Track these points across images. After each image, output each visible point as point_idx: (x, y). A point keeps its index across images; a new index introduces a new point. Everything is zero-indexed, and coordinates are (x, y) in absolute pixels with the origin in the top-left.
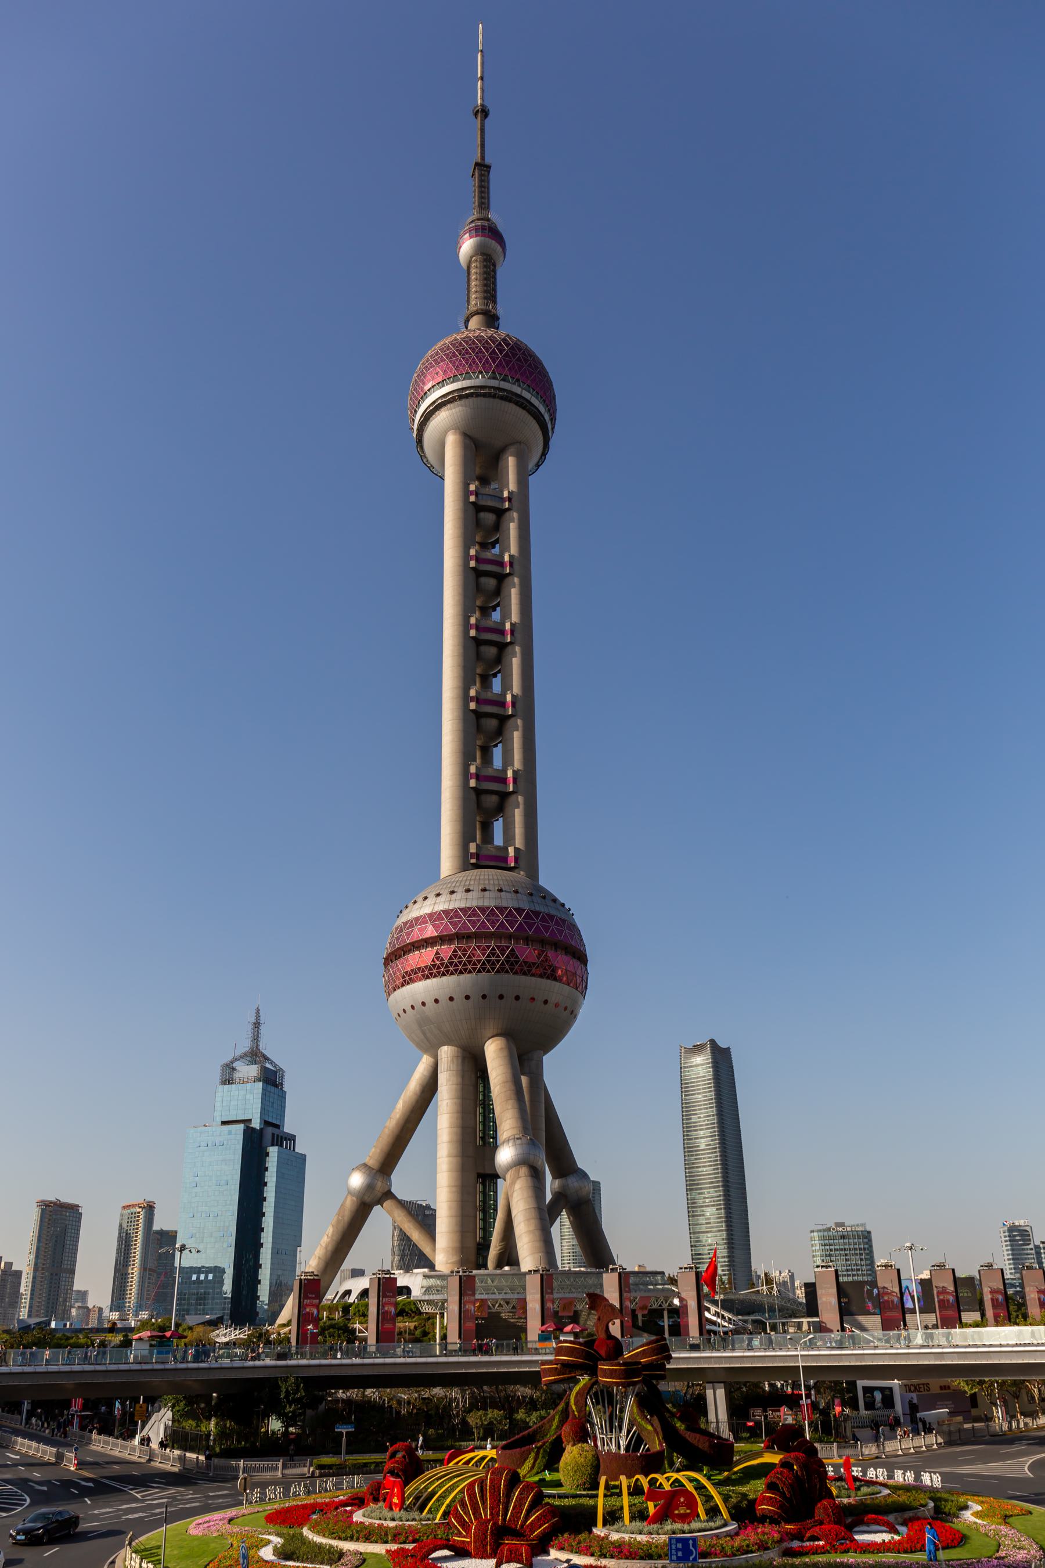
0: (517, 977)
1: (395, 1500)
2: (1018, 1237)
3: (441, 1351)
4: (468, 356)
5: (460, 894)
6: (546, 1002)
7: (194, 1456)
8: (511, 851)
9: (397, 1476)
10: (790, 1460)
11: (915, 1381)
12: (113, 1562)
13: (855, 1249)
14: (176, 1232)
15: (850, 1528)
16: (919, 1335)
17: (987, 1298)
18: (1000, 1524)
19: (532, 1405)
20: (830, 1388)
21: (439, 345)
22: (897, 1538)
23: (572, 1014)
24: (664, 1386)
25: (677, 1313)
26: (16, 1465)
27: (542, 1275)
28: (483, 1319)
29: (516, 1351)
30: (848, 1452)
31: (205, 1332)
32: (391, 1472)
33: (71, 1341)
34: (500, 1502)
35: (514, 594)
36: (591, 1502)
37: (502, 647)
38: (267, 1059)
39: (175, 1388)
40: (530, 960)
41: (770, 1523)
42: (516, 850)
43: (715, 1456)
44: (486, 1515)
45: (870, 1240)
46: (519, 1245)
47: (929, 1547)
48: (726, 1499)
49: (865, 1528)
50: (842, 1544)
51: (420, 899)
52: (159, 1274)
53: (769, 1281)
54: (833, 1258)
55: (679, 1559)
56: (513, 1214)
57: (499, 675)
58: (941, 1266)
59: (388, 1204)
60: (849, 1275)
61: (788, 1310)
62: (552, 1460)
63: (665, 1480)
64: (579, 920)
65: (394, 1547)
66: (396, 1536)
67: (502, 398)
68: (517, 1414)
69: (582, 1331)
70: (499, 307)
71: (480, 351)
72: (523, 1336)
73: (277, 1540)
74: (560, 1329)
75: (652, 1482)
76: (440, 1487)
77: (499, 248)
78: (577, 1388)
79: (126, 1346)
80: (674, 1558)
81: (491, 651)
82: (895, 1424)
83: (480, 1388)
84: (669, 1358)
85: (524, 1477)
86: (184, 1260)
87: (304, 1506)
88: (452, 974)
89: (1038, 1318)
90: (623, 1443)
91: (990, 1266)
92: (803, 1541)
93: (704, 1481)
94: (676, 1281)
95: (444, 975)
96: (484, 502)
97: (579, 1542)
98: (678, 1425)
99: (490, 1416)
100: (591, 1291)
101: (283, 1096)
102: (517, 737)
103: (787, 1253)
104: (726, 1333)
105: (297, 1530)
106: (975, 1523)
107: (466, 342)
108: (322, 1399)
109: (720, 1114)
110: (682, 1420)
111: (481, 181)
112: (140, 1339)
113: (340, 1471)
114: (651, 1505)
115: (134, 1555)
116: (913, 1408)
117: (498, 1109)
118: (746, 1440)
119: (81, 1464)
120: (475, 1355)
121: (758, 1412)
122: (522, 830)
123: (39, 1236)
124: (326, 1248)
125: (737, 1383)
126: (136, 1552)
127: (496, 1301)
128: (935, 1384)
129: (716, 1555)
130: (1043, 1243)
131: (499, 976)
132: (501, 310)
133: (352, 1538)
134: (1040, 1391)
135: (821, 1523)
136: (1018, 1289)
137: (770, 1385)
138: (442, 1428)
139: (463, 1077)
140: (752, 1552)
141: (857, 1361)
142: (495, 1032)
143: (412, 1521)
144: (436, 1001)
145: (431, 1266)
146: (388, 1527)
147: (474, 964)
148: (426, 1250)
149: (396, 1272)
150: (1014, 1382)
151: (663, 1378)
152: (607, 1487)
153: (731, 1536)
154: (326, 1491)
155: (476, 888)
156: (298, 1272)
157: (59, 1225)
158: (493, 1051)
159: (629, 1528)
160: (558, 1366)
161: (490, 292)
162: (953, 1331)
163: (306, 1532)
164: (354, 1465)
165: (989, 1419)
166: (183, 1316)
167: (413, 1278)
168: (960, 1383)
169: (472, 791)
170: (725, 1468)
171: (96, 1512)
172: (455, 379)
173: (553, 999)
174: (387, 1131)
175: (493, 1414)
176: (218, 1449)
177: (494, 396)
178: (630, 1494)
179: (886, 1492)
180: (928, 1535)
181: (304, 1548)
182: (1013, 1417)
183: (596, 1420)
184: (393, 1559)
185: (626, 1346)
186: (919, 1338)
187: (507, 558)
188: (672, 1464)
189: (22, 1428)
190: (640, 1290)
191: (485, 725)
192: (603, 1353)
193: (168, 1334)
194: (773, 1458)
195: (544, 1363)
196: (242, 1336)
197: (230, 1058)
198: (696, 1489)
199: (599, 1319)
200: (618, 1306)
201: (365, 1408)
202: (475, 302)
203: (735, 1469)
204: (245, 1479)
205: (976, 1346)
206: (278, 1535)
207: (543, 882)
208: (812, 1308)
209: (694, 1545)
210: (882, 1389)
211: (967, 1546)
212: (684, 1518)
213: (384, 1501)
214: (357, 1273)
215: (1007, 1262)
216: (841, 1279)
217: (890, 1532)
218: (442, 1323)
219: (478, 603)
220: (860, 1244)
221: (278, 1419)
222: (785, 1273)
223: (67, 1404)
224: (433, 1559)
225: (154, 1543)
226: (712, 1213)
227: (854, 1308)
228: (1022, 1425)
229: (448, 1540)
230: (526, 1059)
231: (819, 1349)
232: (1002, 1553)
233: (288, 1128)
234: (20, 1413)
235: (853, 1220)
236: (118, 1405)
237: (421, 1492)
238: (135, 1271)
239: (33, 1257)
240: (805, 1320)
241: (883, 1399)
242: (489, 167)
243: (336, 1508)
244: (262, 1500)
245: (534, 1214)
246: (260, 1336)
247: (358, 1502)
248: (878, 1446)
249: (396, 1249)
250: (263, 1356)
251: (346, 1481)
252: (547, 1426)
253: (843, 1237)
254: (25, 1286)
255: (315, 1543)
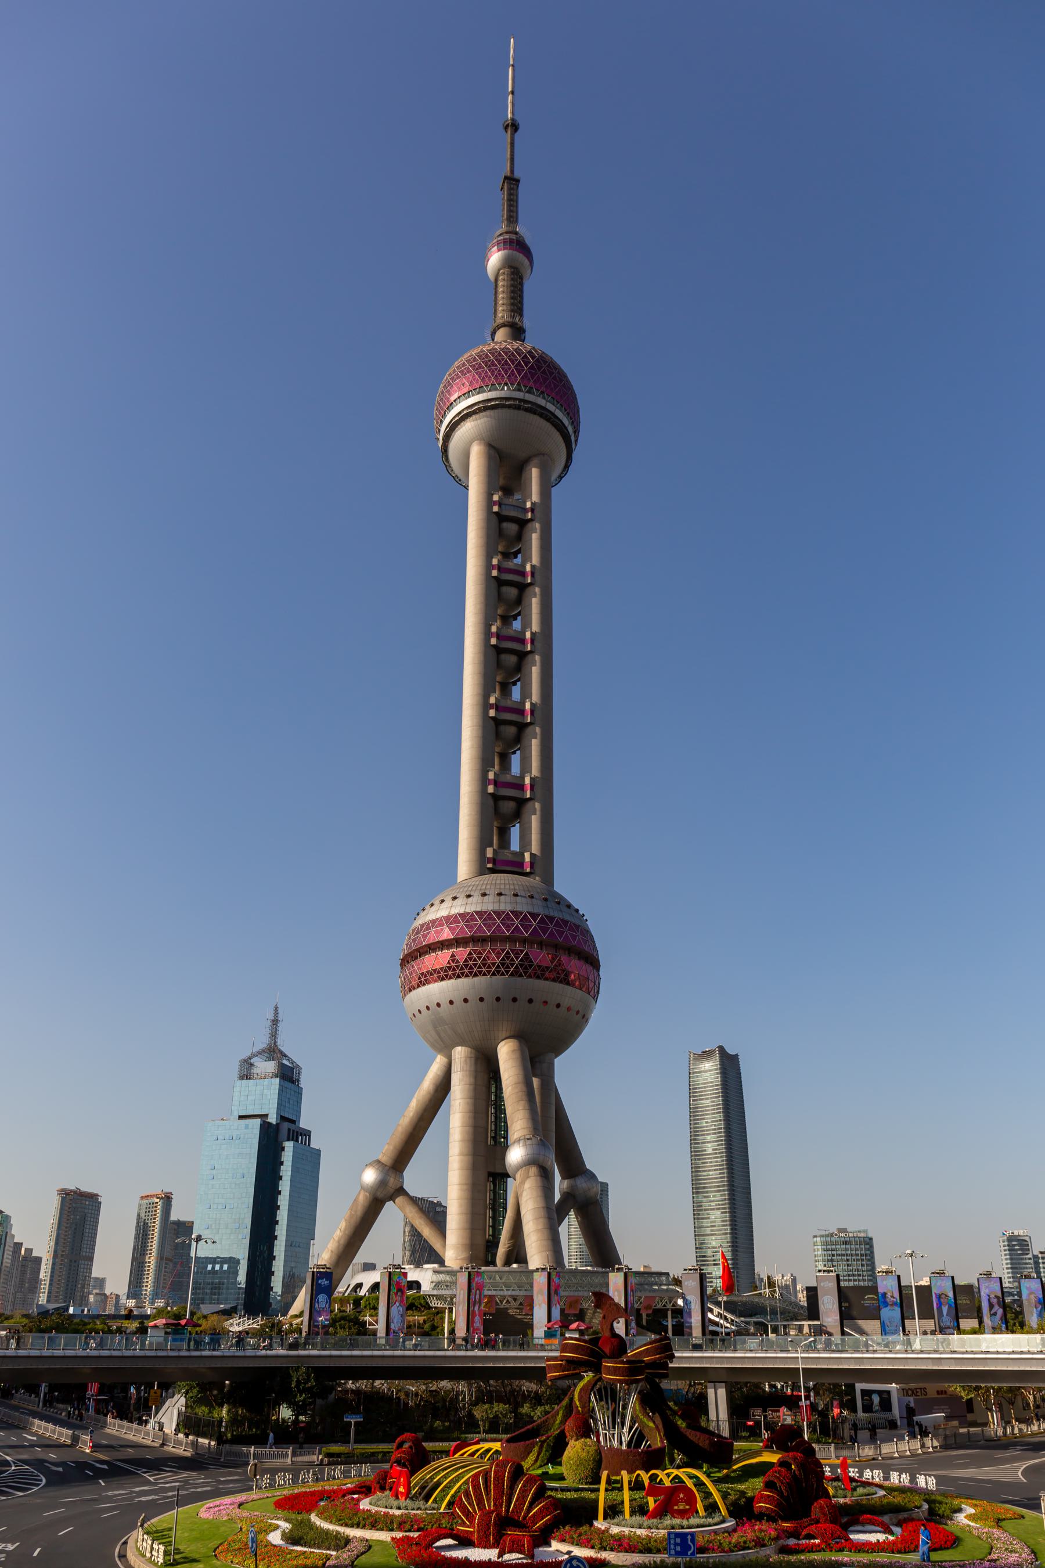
0: (531, 980)
1: (401, 1489)
2: (1017, 1246)
3: (449, 1346)
4: (494, 367)
5: (476, 898)
6: (558, 1006)
7: (206, 1441)
8: (527, 855)
9: (404, 1466)
10: (787, 1459)
11: (912, 1385)
12: (125, 1543)
13: (857, 1255)
14: (193, 1223)
15: (846, 1528)
16: (918, 1340)
17: (985, 1305)
18: (993, 1527)
19: (537, 1400)
20: (829, 1390)
21: (466, 356)
22: (891, 1538)
23: (584, 1018)
24: (666, 1385)
25: (678, 1312)
26: (32, 1446)
27: (549, 1274)
28: (491, 1315)
29: (522, 1346)
30: (845, 1453)
31: (219, 1321)
32: (398, 1462)
33: (89, 1327)
34: (504, 1494)
35: (535, 603)
36: (593, 1496)
37: (522, 656)
38: (285, 1055)
39: (188, 1375)
40: (544, 964)
41: (767, 1521)
42: (532, 855)
43: (715, 1454)
44: (489, 1506)
45: (872, 1247)
46: (527, 1243)
47: (923, 1548)
48: (725, 1496)
49: (860, 1528)
50: (837, 1543)
52: (175, 1264)
53: (771, 1284)
54: (835, 1263)
55: (677, 1553)
56: (522, 1214)
57: (519, 683)
58: (941, 1274)
59: (400, 1200)
60: (850, 1280)
61: (789, 1313)
62: (556, 1454)
63: (665, 1477)
64: (593, 926)
65: (399, 1535)
66: (402, 1524)
67: (526, 410)
68: (520, 1407)
69: (588, 1328)
70: (525, 320)
71: (506, 363)
72: (529, 1332)
73: (285, 1525)
74: (565, 1325)
75: (654, 1477)
76: (445, 1477)
77: (526, 262)
78: (581, 1384)
79: (142, 1333)
80: (673, 1552)
81: (512, 659)
82: (893, 1425)
83: (486, 1382)
84: (672, 1357)
85: (528, 1469)
86: (200, 1251)
87: (313, 1493)
88: (467, 976)
89: (1035, 1325)
90: (625, 1439)
91: (988, 1274)
92: (799, 1539)
93: (703, 1478)
94: (680, 1282)
95: (459, 977)
96: (505, 513)
97: (580, 1535)
98: (679, 1423)
99: (496, 1409)
100: (597, 1290)
101: (299, 1093)
102: (535, 744)
103: (789, 1257)
104: (728, 1334)
105: (305, 1516)
106: (969, 1526)
107: (493, 354)
108: (333, 1389)
109: (727, 1119)
110: (683, 1417)
111: (510, 194)
112: (156, 1326)
113: (348, 1459)
114: (651, 1500)
115: (146, 1537)
116: (910, 1412)
117: (509, 1110)
118: (746, 1439)
119: (96, 1447)
120: (483, 1350)
121: (758, 1412)
123: (59, 1223)
124: (339, 1242)
125: (737, 1383)
126: (148, 1533)
127: (504, 1297)
128: (932, 1388)
129: (713, 1550)
130: (1041, 1253)
131: (513, 979)
133: (358, 1526)
134: (1035, 1398)
135: (817, 1522)
136: (1016, 1297)
137: (771, 1386)
138: (449, 1421)
139: (476, 1078)
140: (749, 1548)
141: (856, 1364)
142: (508, 1035)
143: (418, 1510)
144: (451, 1002)
145: (441, 1262)
146: (393, 1515)
147: (489, 967)
148: (437, 1245)
149: (407, 1267)
150: (1009, 1389)
151: (666, 1376)
152: (609, 1482)
153: (729, 1533)
154: (334, 1478)
155: (492, 892)
156: (311, 1265)
157: (79, 1214)
158: (506, 1053)
159: (629, 1522)
160: (563, 1363)
161: (516, 305)
162: (951, 1337)
163: (314, 1518)
164: (362, 1454)
165: (986, 1424)
166: (198, 1305)
167: (423, 1273)
168: (956, 1388)
169: (490, 797)
170: (724, 1466)
171: (110, 1493)
172: (481, 390)
173: (566, 1002)
174: (400, 1129)
175: (499, 1408)
176: (229, 1436)
177: (518, 408)
178: (630, 1489)
179: (882, 1493)
180: (922, 1537)
181: (311, 1534)
182: (1008, 1422)
183: (599, 1416)
184: (398, 1547)
185: (630, 1345)
186: (917, 1346)
187: (528, 568)
188: (672, 1461)
189: (39, 1410)
190: (645, 1290)
191: (504, 731)
192: (607, 1351)
193: (183, 1322)
194: (772, 1457)
195: (549, 1359)
196: (255, 1326)
197: (249, 1054)
198: (695, 1485)
199: (604, 1317)
200: (623, 1305)
201: (373, 1399)
202: (502, 314)
203: (735, 1467)
204: (256, 1465)
205: (972, 1352)
206: (287, 1520)
207: (558, 887)
208: (813, 1311)
209: (693, 1540)
210: (880, 1393)
211: (960, 1548)
212: (683, 1514)
213: (390, 1490)
214: (369, 1267)
215: (1006, 1271)
216: (842, 1284)
217: (884, 1532)
218: (450, 1317)
219: (499, 612)
220: (861, 1249)
221: (289, 1407)
222: (788, 1277)
223: (84, 1388)
224: (436, 1548)
225: (165, 1525)
226: (717, 1216)
227: (855, 1313)
228: (1016, 1431)
229: (453, 1529)
230: (538, 1060)
231: (819, 1352)
232: (994, 1556)
233: (303, 1124)
234: (38, 1395)
235: (855, 1226)
236: (133, 1390)
237: (426, 1482)
238: (152, 1260)
239: (52, 1244)
240: (806, 1323)
241: (880, 1403)
242: (518, 181)
243: (344, 1496)
244: (271, 1486)
245: (542, 1213)
246: (273, 1325)
247: (365, 1490)
248: (875, 1448)
249: (407, 1244)
250: (275, 1345)
251: (353, 1470)
252: (552, 1421)
253: (845, 1243)
254: (45, 1272)
255: (322, 1530)
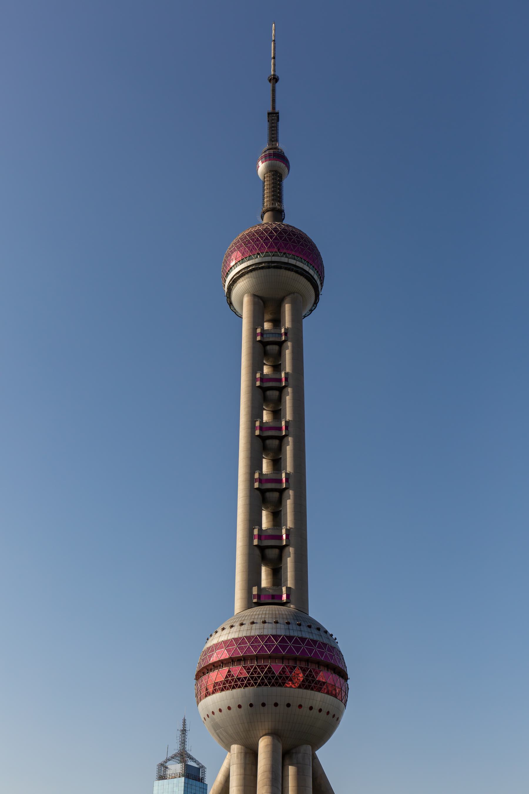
0: (274, 688)
42: (288, 589)
51: (219, 630)
77: (282, 165)
107: (267, 232)
122: (293, 573)
132: (287, 205)
139: (245, 769)
144: (229, 708)
147: (256, 679)
161: (277, 194)
